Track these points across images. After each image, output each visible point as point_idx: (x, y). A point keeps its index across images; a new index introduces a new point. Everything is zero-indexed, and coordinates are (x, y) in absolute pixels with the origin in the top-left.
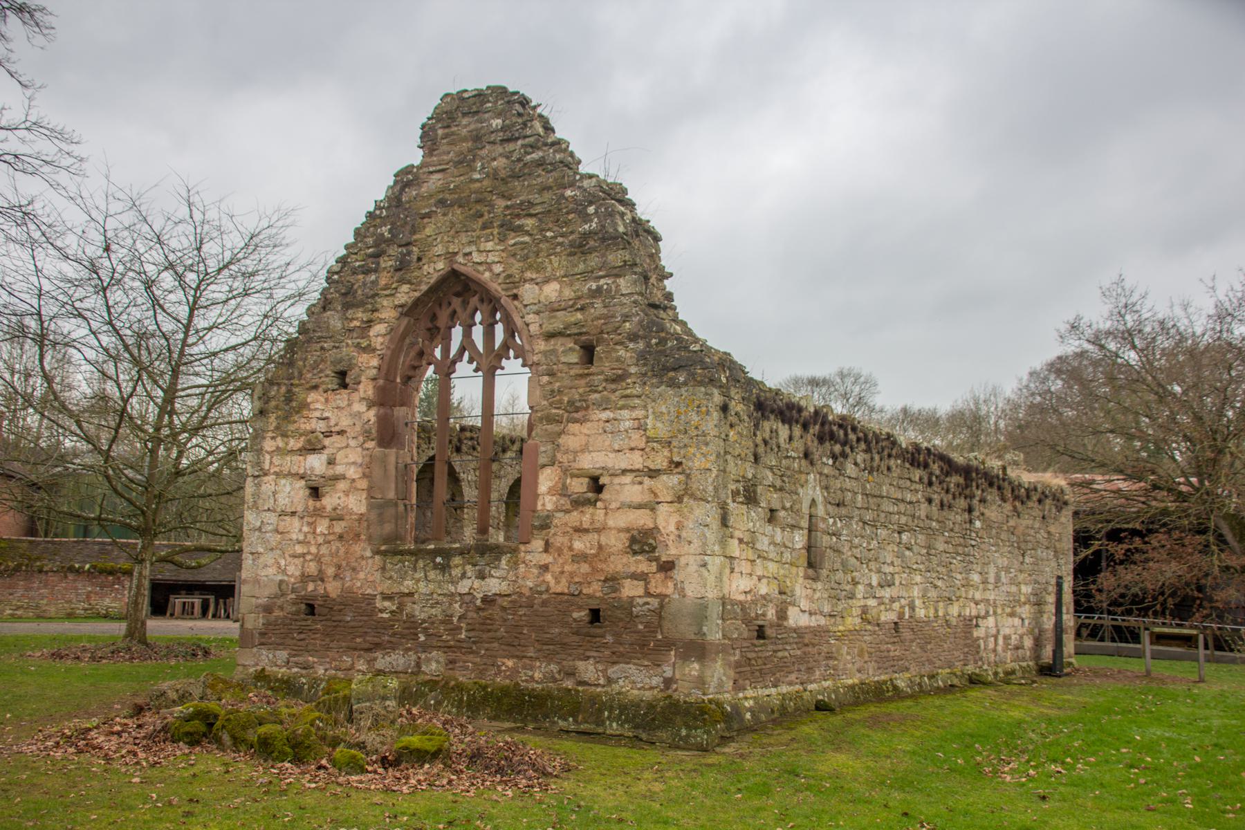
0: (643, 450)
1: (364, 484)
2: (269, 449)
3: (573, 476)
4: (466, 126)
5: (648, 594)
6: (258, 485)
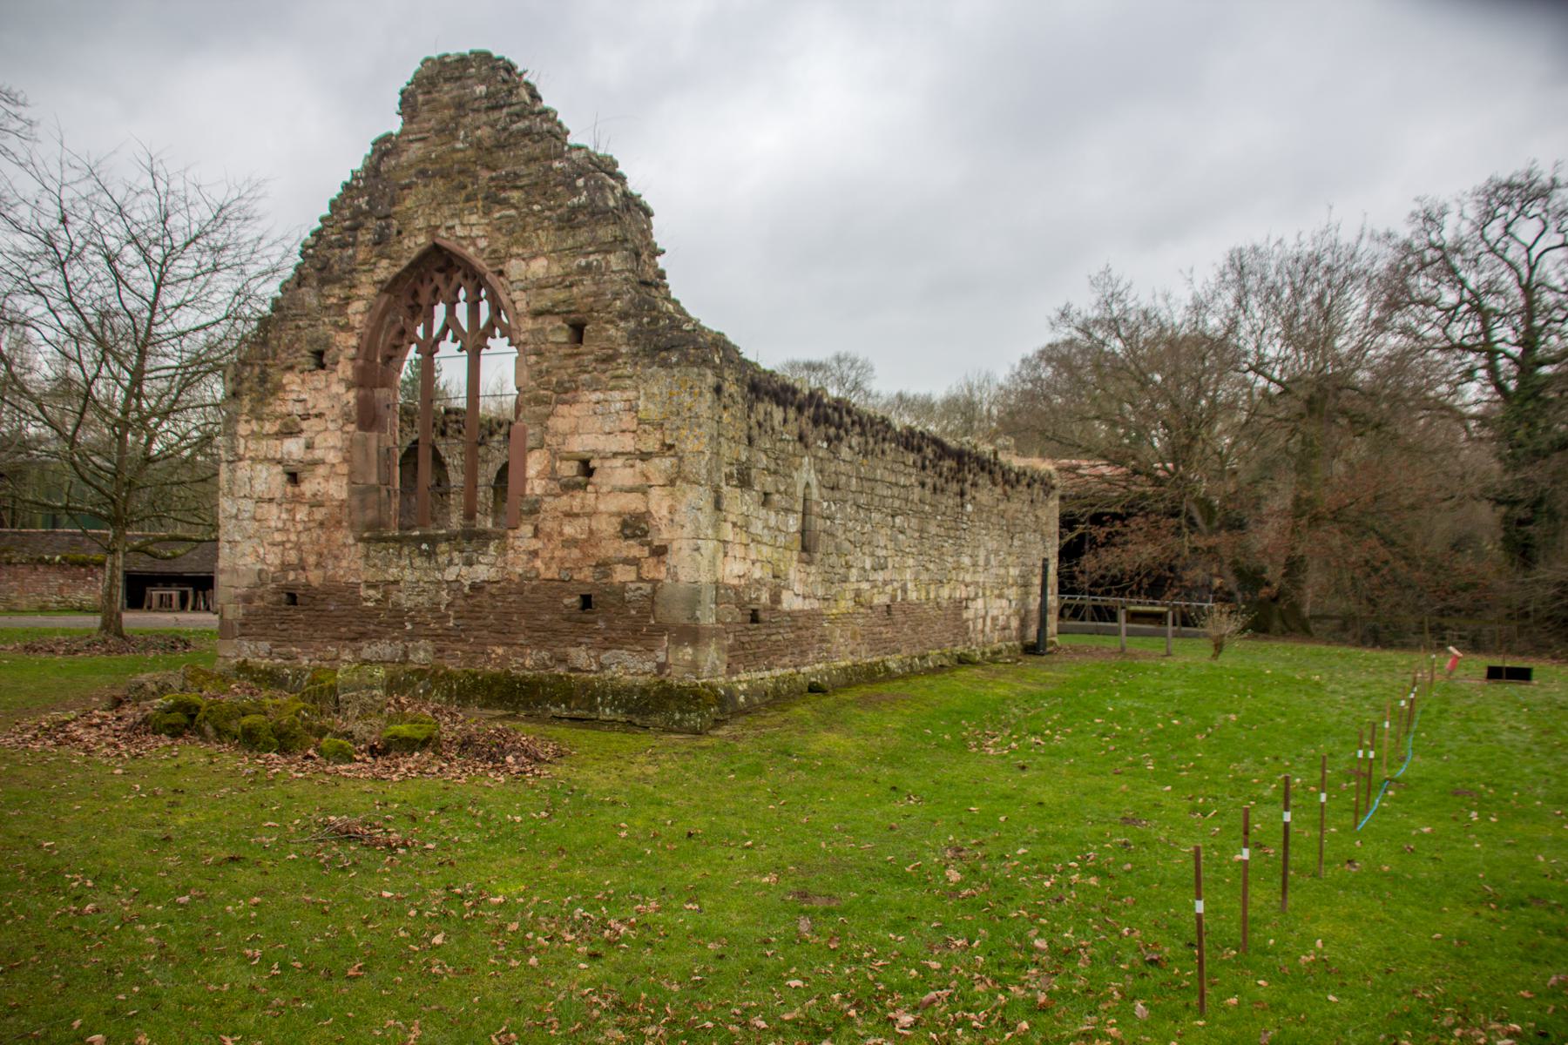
0: (634, 432)
1: (344, 469)
2: (244, 433)
3: (562, 459)
4: (447, 92)
5: (640, 579)
6: (233, 471)
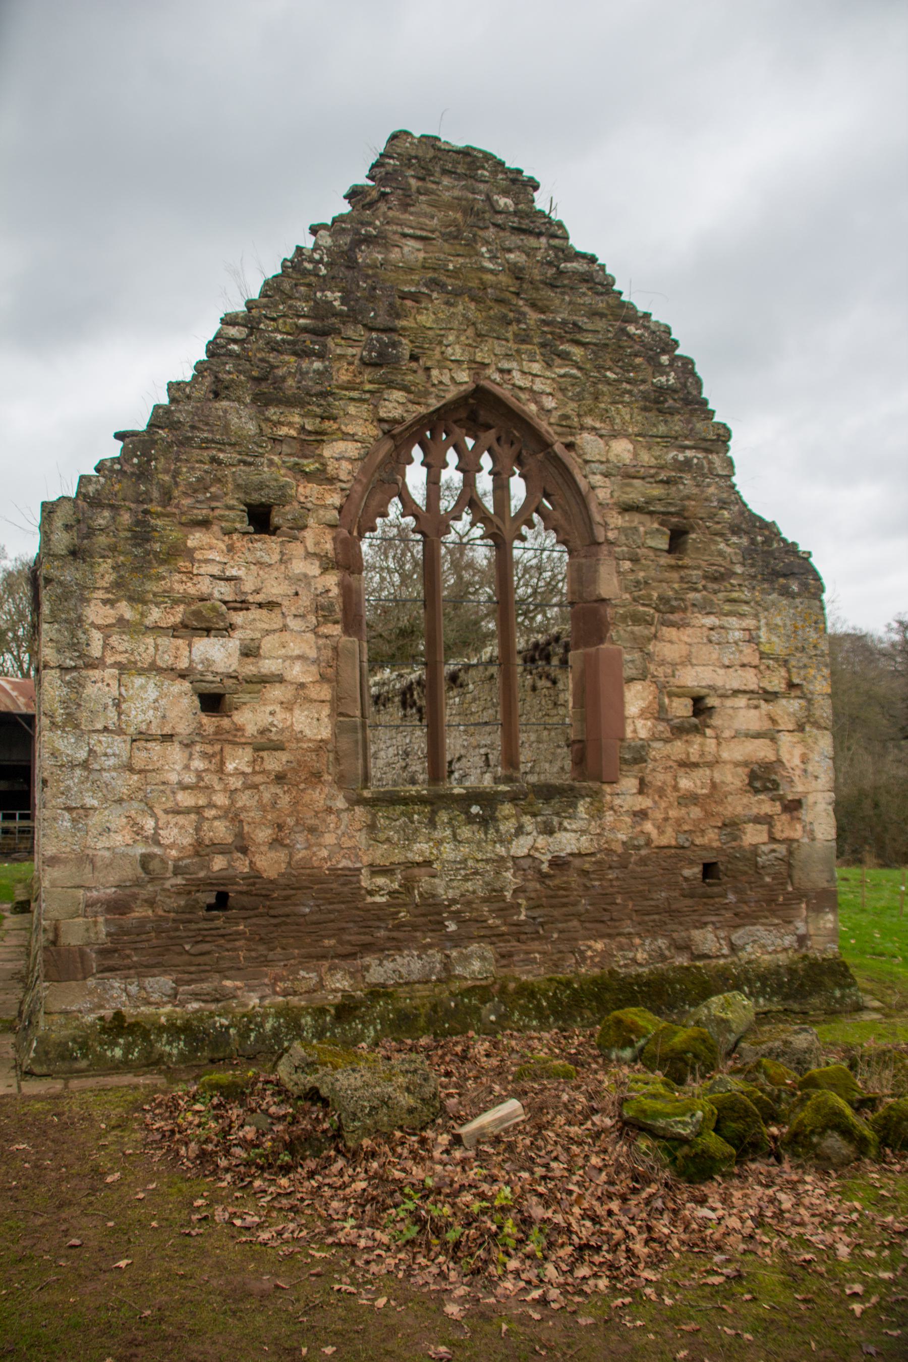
0: (755, 667)
1: (325, 692)
3: (671, 695)
5: (773, 839)
6: (76, 686)
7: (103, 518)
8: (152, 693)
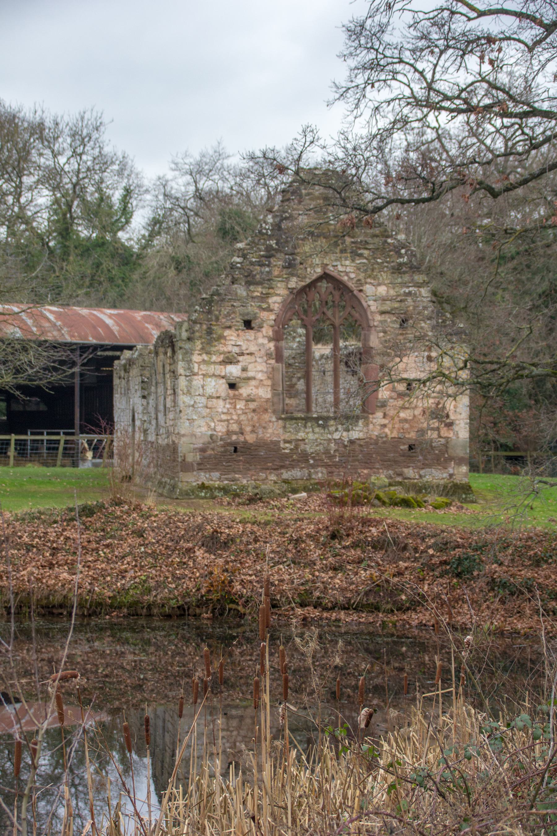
1: (269, 382)
6: (190, 381)
7: (197, 327)
8: (213, 383)
